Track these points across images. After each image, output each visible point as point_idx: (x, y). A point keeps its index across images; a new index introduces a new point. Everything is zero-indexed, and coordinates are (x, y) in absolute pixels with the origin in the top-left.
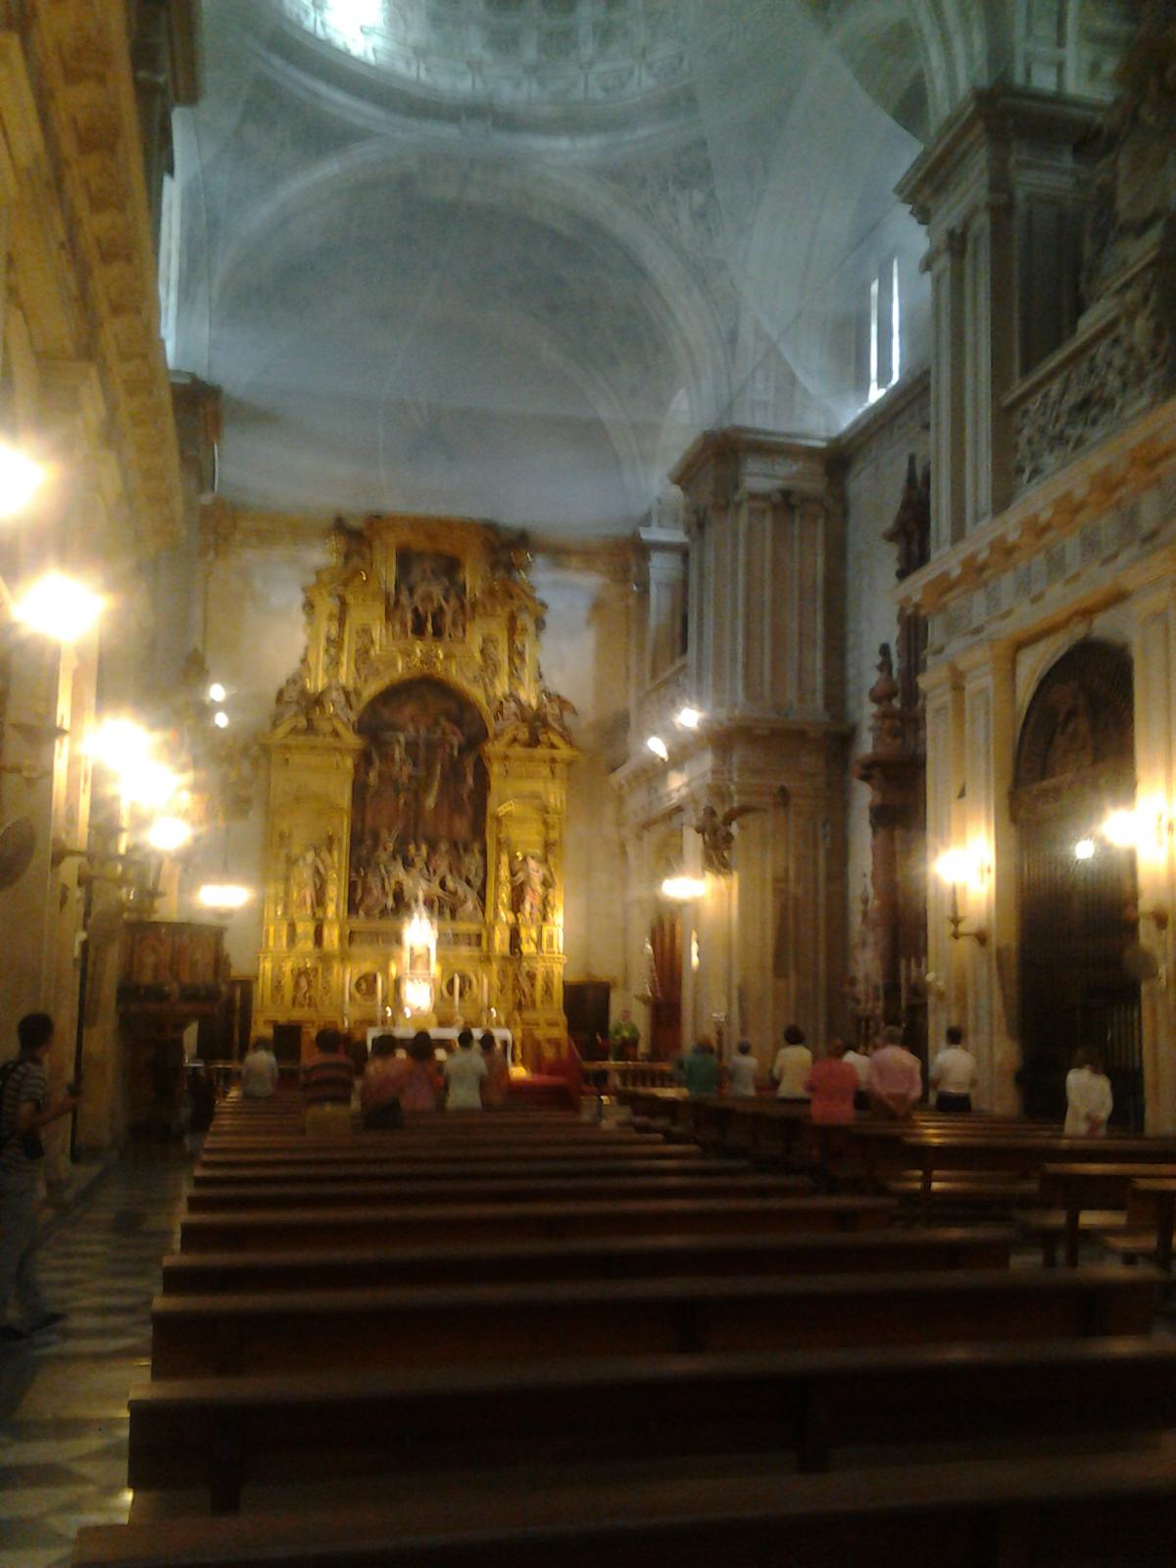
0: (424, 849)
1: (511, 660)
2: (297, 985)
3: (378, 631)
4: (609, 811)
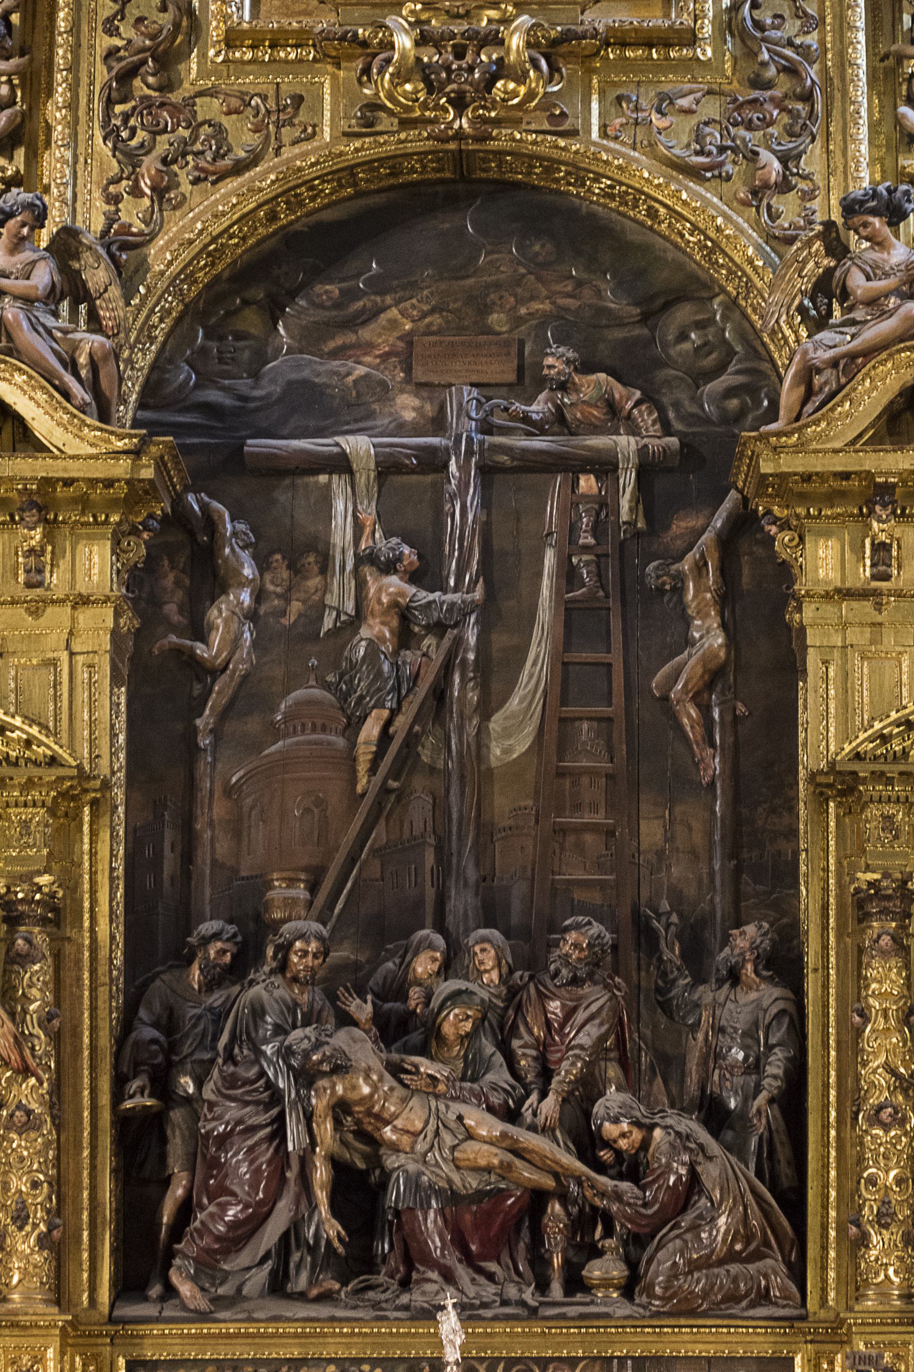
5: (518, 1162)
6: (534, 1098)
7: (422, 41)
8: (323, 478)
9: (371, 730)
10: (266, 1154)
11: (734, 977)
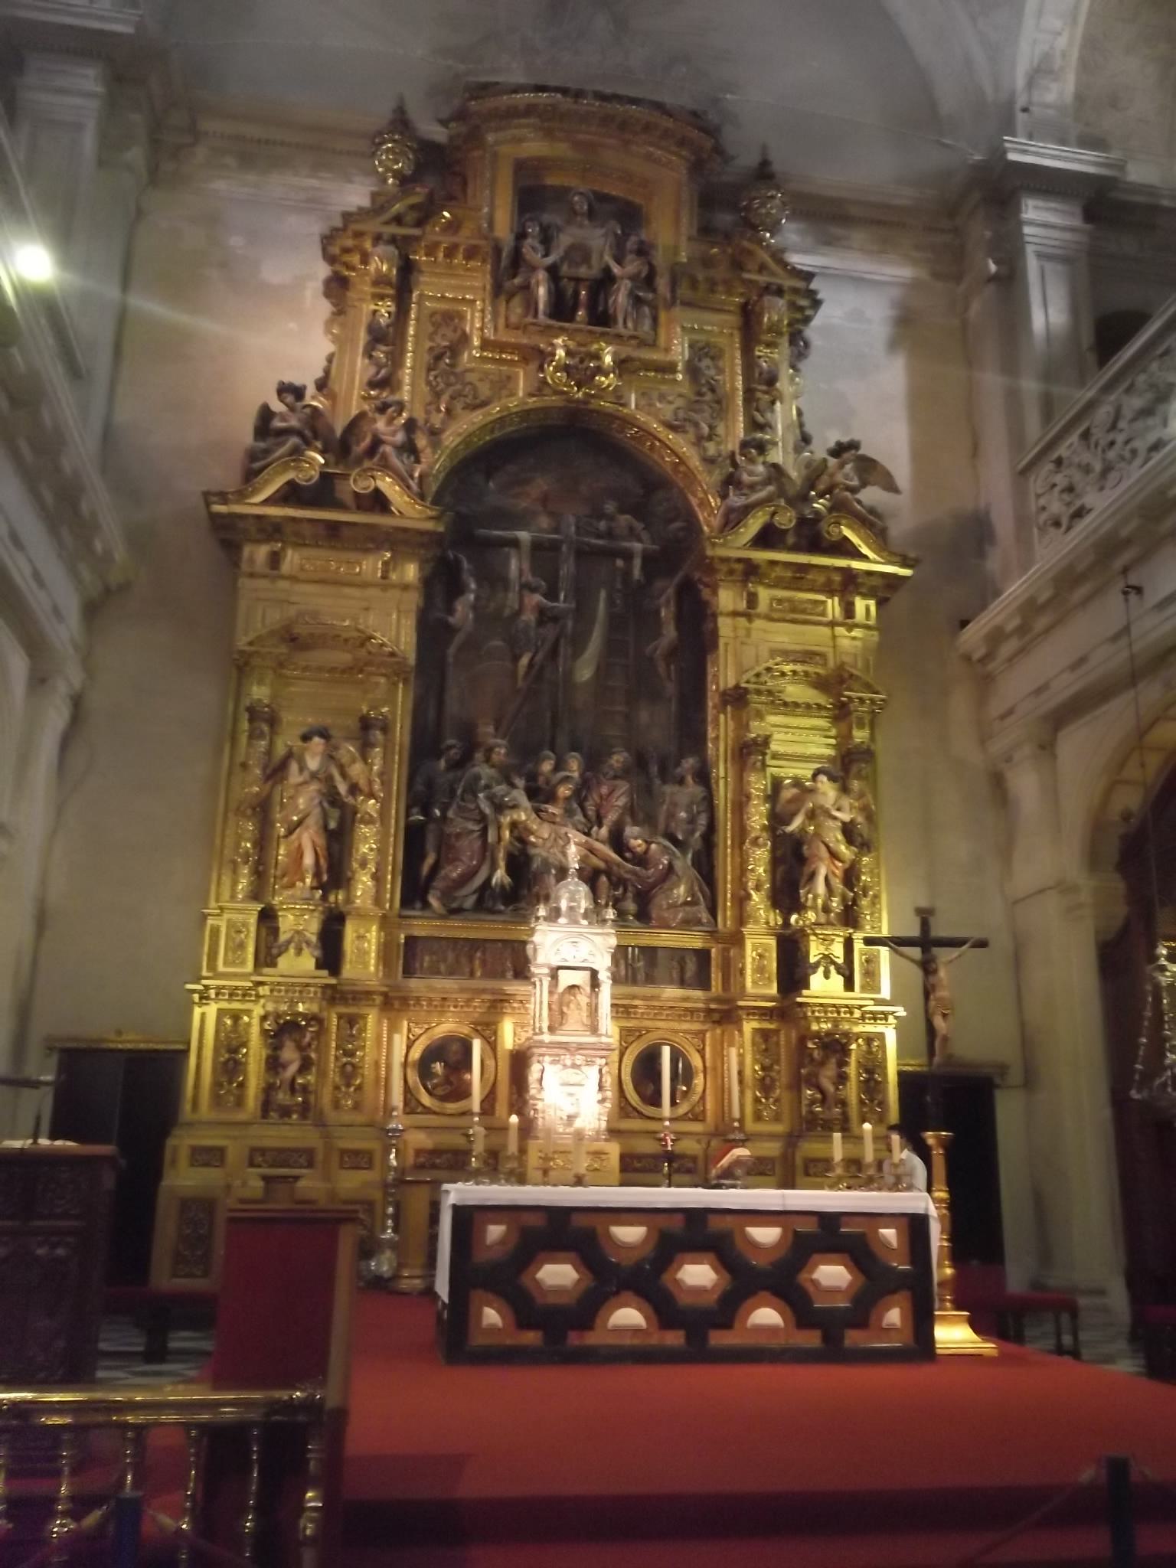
0: (574, 766)
1: (749, 394)
2: (274, 1064)
3: (477, 322)
4: (960, 705)
5: (591, 855)
6: (595, 828)
7: (569, 353)
8: (506, 549)
9: (525, 661)
10: (478, 844)
11: (681, 781)
